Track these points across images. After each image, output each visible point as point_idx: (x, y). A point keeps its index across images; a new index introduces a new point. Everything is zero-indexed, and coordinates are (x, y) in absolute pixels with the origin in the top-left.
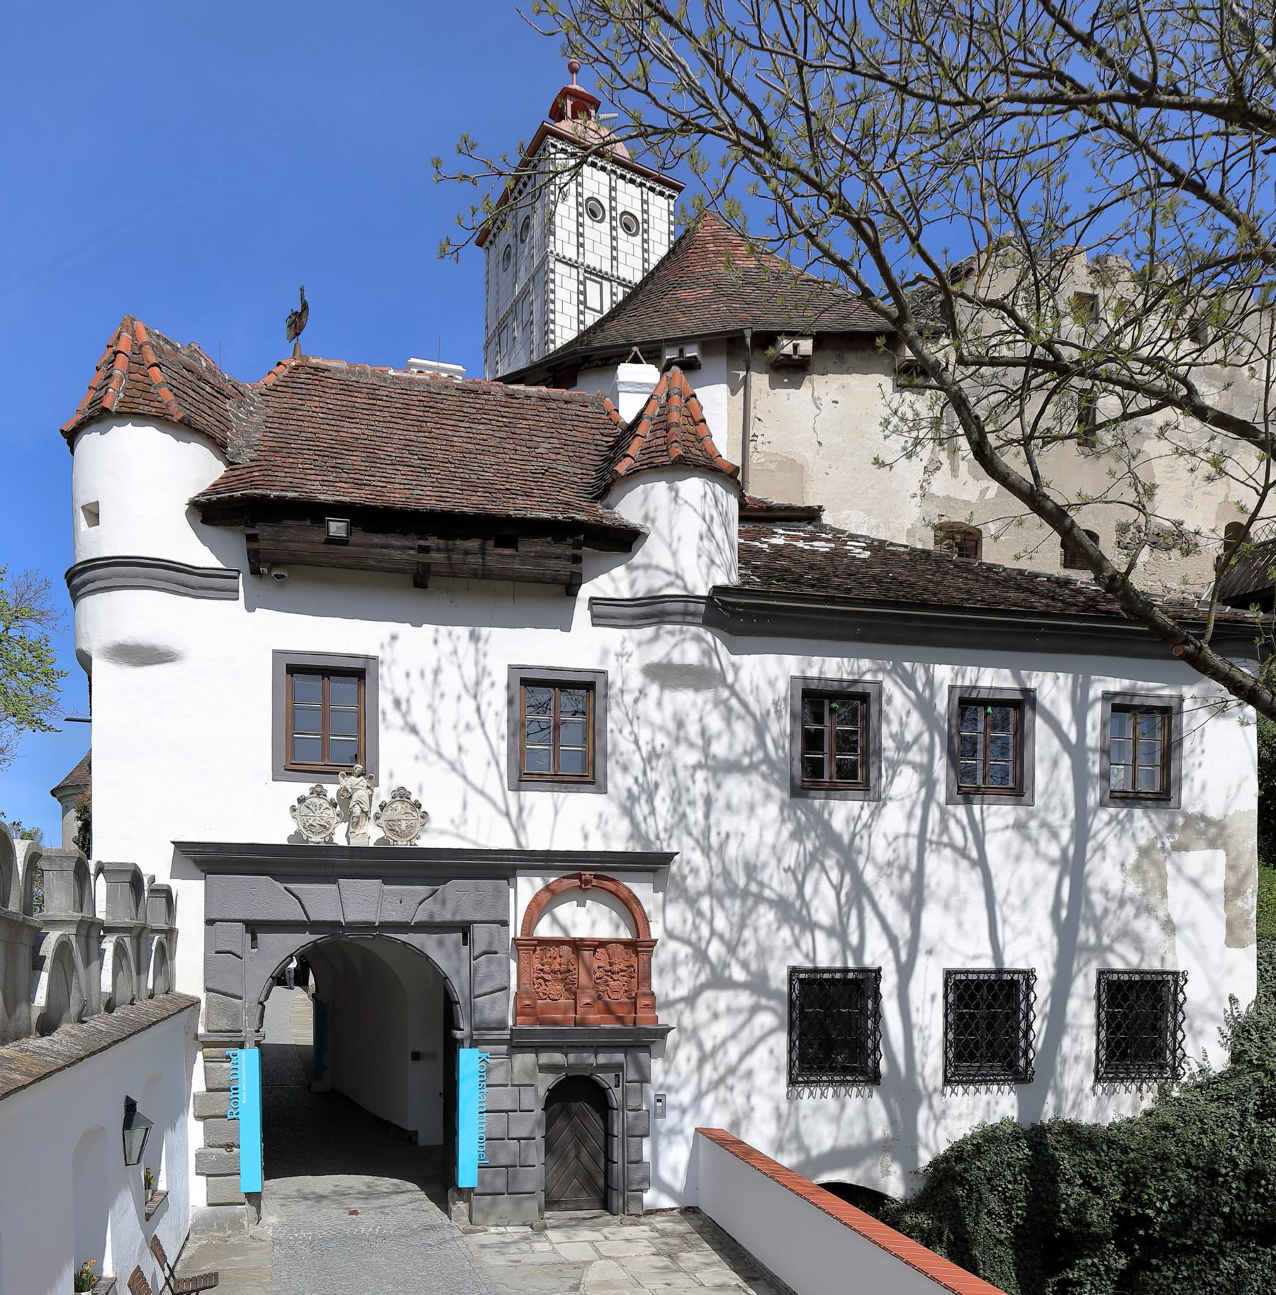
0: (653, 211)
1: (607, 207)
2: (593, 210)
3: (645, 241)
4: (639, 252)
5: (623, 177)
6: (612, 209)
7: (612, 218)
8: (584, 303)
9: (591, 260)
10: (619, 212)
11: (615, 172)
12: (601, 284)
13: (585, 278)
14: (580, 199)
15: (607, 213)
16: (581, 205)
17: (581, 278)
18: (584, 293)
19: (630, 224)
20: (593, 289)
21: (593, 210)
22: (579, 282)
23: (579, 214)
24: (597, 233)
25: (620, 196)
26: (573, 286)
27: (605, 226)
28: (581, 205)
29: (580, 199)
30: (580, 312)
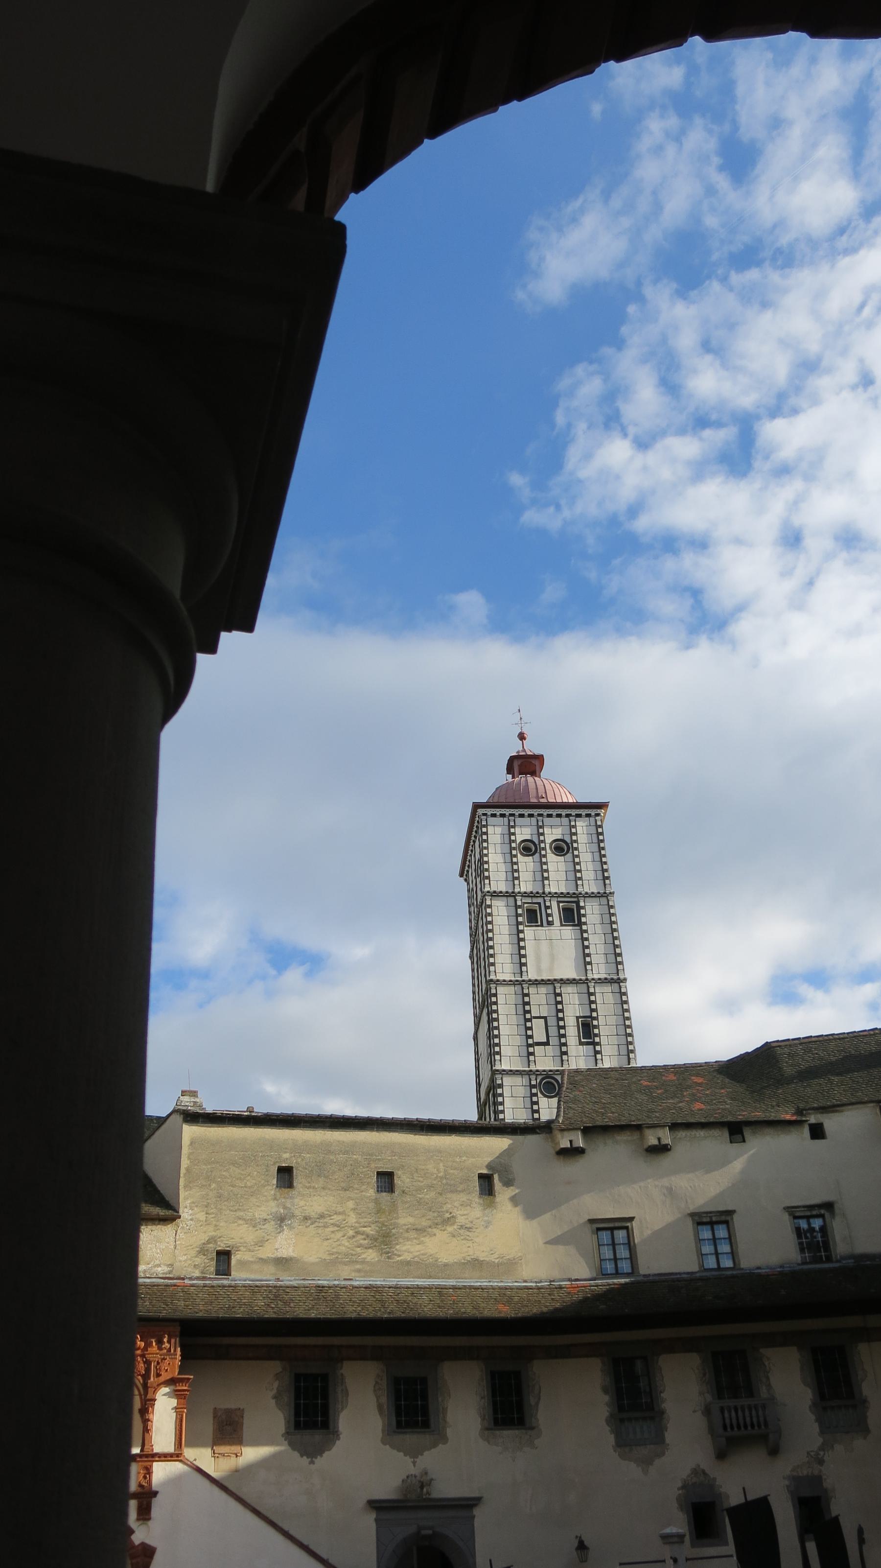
3: (574, 856)
7: (544, 849)
14: (513, 845)
16: (514, 849)
23: (512, 856)
28: (514, 849)
29: (513, 845)
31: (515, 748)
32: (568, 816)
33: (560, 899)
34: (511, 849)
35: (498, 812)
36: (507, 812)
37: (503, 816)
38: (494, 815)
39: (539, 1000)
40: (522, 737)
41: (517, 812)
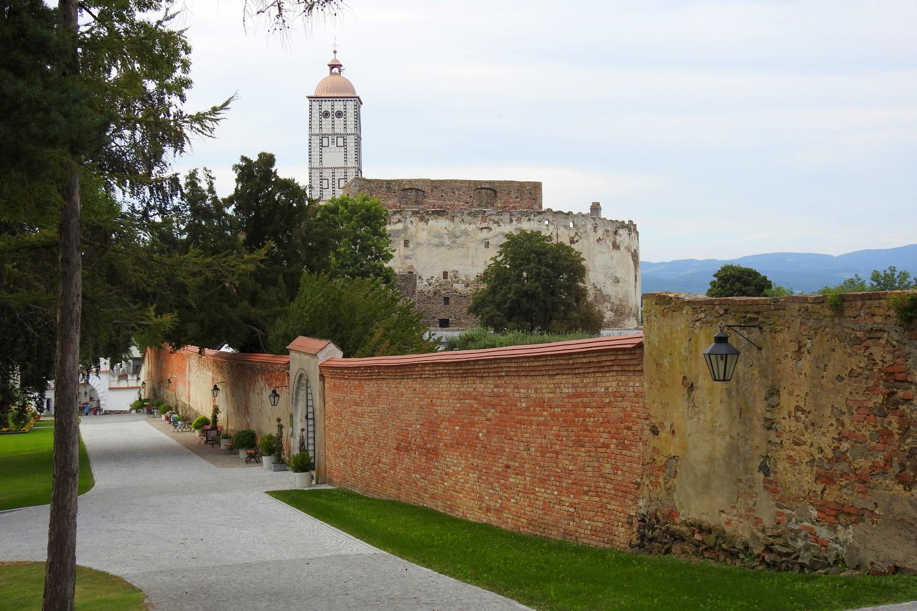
0: (348, 107)
1: (330, 112)
2: (326, 114)
4: (342, 123)
5: (336, 101)
9: (325, 131)
10: (335, 112)
18: (322, 143)
19: (339, 114)
20: (325, 140)
21: (326, 114)
24: (327, 122)
25: (336, 107)
26: (318, 141)
27: (330, 119)
31: (330, 59)
35: (316, 99)
36: (320, 99)
39: (327, 174)
40: (335, 52)
41: (323, 99)
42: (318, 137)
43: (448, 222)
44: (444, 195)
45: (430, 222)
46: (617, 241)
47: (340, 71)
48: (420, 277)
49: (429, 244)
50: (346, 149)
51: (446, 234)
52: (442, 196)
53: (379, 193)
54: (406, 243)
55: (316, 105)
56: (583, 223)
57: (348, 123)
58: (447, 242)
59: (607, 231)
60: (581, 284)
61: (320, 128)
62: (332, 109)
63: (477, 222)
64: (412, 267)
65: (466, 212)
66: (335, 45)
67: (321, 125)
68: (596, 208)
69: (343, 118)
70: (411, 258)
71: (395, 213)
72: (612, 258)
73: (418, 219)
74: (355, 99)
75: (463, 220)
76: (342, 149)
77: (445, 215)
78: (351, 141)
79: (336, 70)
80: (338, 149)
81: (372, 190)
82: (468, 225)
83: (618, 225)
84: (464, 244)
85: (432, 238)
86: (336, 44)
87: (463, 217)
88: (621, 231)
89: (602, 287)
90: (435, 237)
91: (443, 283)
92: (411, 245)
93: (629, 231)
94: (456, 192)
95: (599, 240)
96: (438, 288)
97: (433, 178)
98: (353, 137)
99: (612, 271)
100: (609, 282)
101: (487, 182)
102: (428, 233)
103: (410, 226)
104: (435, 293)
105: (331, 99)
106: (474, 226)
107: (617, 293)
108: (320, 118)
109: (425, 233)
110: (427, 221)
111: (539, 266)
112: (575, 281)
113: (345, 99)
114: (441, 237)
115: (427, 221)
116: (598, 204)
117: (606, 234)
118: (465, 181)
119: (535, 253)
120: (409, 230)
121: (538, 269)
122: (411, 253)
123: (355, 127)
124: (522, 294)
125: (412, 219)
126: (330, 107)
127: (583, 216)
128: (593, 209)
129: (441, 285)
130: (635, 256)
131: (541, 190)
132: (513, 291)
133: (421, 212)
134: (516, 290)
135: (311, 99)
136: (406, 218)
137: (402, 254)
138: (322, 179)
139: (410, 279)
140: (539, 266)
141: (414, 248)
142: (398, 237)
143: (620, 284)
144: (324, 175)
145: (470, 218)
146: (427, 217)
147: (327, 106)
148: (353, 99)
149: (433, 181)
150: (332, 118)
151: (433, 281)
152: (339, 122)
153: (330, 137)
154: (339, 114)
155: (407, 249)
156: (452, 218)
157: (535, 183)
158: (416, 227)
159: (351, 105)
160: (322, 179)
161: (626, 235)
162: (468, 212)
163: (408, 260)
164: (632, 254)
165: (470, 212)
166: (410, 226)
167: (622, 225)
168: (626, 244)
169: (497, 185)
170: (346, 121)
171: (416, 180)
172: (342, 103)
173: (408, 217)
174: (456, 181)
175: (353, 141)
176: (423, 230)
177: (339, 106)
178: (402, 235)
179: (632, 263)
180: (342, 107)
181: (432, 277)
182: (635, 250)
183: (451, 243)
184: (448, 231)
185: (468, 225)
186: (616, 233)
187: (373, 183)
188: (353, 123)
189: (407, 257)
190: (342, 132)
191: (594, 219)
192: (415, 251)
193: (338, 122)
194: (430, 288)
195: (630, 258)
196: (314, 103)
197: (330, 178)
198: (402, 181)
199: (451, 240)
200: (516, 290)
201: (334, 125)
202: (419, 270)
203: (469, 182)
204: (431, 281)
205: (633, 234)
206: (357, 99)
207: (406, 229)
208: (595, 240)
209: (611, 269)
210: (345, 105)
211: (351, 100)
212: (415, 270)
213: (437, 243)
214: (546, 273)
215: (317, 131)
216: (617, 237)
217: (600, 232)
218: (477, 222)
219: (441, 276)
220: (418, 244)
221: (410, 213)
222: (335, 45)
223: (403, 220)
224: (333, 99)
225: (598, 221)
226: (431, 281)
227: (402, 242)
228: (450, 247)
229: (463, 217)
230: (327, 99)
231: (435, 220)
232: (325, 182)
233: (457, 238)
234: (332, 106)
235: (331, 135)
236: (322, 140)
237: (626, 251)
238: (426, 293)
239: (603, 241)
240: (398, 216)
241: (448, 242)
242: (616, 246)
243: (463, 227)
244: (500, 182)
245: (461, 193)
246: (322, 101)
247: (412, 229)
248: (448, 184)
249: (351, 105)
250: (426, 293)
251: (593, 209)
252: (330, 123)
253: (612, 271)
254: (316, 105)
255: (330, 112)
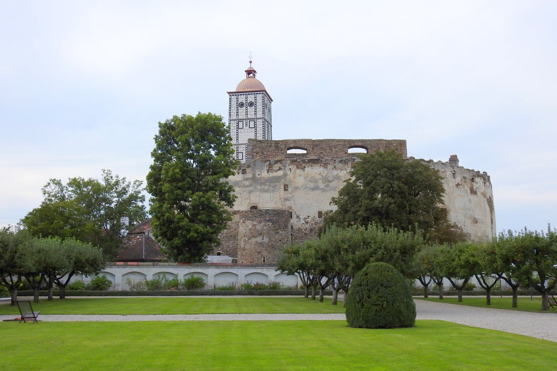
1: (245, 103)
2: (242, 105)
3: (255, 107)
4: (253, 110)
5: (249, 94)
6: (246, 103)
7: (246, 105)
8: (238, 128)
9: (240, 117)
10: (248, 103)
11: (246, 94)
12: (243, 122)
13: (238, 122)
15: (245, 104)
17: (237, 122)
18: (238, 126)
19: (251, 104)
20: (241, 124)
21: (242, 105)
22: (237, 123)
24: (242, 110)
26: (235, 125)
27: (244, 108)
29: (237, 104)
30: (237, 130)
32: (254, 94)
33: (250, 120)
34: (237, 105)
35: (234, 94)
37: (235, 95)
38: (233, 95)
40: (251, 62)
42: (235, 121)
43: (322, 168)
44: (323, 151)
45: (306, 169)
46: (474, 187)
47: (254, 75)
48: (298, 217)
49: (306, 188)
50: (256, 129)
51: (320, 179)
52: (322, 153)
53: (269, 151)
54: (286, 188)
55: (234, 98)
56: (443, 170)
57: (257, 110)
58: (322, 186)
59: (465, 178)
60: (440, 205)
61: (237, 115)
62: (246, 100)
63: (347, 168)
64: (291, 208)
65: (337, 160)
66: (251, 57)
67: (238, 112)
68: (454, 159)
69: (254, 106)
70: (290, 200)
71: (276, 162)
72: (470, 201)
73: (295, 167)
74: (263, 92)
75: (335, 167)
76: (253, 130)
77: (319, 163)
78: (260, 123)
79: (251, 75)
80: (250, 130)
81: (263, 149)
82: (339, 171)
83: (474, 174)
84: (335, 188)
85: (308, 183)
86: (252, 56)
87: (335, 164)
88: (477, 179)
89: (463, 227)
90: (311, 182)
91: (319, 222)
92: (290, 189)
93: (484, 180)
94: (334, 149)
95: (458, 185)
96: (314, 226)
97: (313, 139)
98: (261, 120)
99: (471, 212)
100: (468, 222)
101: (359, 141)
102: (305, 178)
103: (289, 172)
104: (311, 230)
105: (245, 94)
106: (345, 172)
107: (476, 232)
108: (237, 108)
109: (302, 178)
110: (303, 168)
111: (391, 181)
112: (432, 202)
113: (256, 93)
114: (316, 181)
115: (303, 168)
116: (456, 156)
117: (464, 180)
118: (341, 140)
119: (387, 168)
120: (288, 176)
121: (390, 183)
122: (290, 196)
123: (263, 113)
124: (373, 212)
125: (291, 167)
126: (244, 99)
127: (442, 164)
128: (452, 161)
129: (316, 223)
130: (490, 202)
131: (406, 146)
132: (363, 208)
133: (298, 160)
134: (366, 207)
135: (230, 94)
136: (285, 166)
137: (282, 196)
138: (238, 153)
139: (282, 214)
140: (391, 181)
141: (292, 192)
142: (279, 182)
143: (478, 225)
144: (239, 149)
145: (341, 165)
146: (303, 165)
147: (242, 99)
148: (261, 93)
149: (315, 141)
150: (246, 107)
151: (309, 220)
152: (251, 110)
153: (244, 121)
154: (251, 104)
155: (286, 192)
156: (325, 165)
157: (400, 141)
158: (294, 173)
159: (259, 97)
160: (238, 153)
161: (481, 183)
162: (339, 160)
163: (288, 202)
164: (487, 199)
165: (341, 159)
166: (289, 172)
167: (478, 174)
168: (482, 190)
169: (368, 143)
170: (256, 109)
171: (299, 140)
172: (253, 96)
173: (287, 165)
174: (333, 140)
175: (262, 123)
176: (300, 176)
177: (251, 98)
178: (282, 181)
179: (488, 208)
180: (253, 99)
181: (308, 216)
182: (490, 197)
183: (325, 186)
184: (322, 176)
185: (339, 171)
186: (473, 180)
187: (264, 143)
188: (261, 110)
189: (287, 199)
190: (253, 117)
191: (453, 167)
192: (293, 194)
193: (251, 110)
194: (307, 226)
195: (486, 203)
196: (232, 97)
197: (244, 152)
198: (288, 141)
199: (325, 184)
200: (366, 207)
201: (247, 112)
202: (296, 209)
203: (344, 141)
204: (308, 220)
205: (487, 184)
206: (264, 92)
207: (285, 175)
208: (454, 185)
209: (470, 210)
210: (256, 97)
211: (260, 94)
212: (293, 210)
213: (312, 187)
214: (400, 187)
215: (235, 117)
216: (474, 184)
217: (458, 179)
218: (347, 168)
219: (317, 215)
220: (296, 188)
221: (289, 162)
222: (251, 57)
223: (283, 167)
224: (246, 93)
225: (456, 169)
226: (308, 220)
227: (282, 187)
228: (323, 190)
229: (335, 164)
230: (242, 94)
231: (310, 167)
232: (240, 155)
233: (331, 182)
234: (246, 98)
235: (245, 119)
236: (238, 123)
237: (482, 196)
238: (303, 230)
239: (462, 186)
240: (279, 165)
241: (322, 186)
242: (473, 192)
243: (335, 172)
244: (371, 141)
245: (337, 150)
246: (238, 95)
247: (290, 175)
248: (326, 143)
249: (259, 97)
250: (303, 230)
251: (452, 161)
252: (245, 111)
253: (471, 212)
254: (234, 98)
255: (245, 103)
